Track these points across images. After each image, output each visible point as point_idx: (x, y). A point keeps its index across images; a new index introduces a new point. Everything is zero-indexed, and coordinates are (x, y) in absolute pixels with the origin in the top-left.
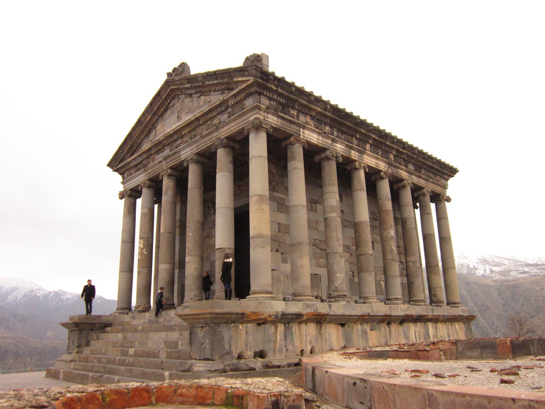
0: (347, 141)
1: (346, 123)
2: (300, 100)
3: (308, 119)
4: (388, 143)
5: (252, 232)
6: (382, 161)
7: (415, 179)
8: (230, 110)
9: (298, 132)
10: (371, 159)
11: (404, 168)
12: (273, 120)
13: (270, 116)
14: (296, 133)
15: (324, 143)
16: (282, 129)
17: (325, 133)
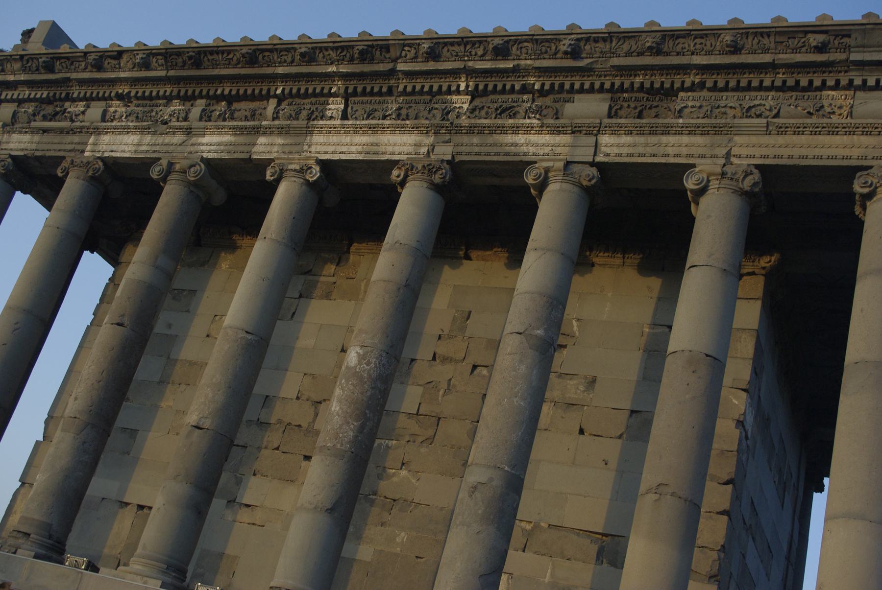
1: (216, 72)
2: (74, 76)
3: (117, 107)
4: (401, 67)
6: (402, 130)
10: (347, 139)
13: (16, 137)
15: (157, 148)
17: (165, 123)
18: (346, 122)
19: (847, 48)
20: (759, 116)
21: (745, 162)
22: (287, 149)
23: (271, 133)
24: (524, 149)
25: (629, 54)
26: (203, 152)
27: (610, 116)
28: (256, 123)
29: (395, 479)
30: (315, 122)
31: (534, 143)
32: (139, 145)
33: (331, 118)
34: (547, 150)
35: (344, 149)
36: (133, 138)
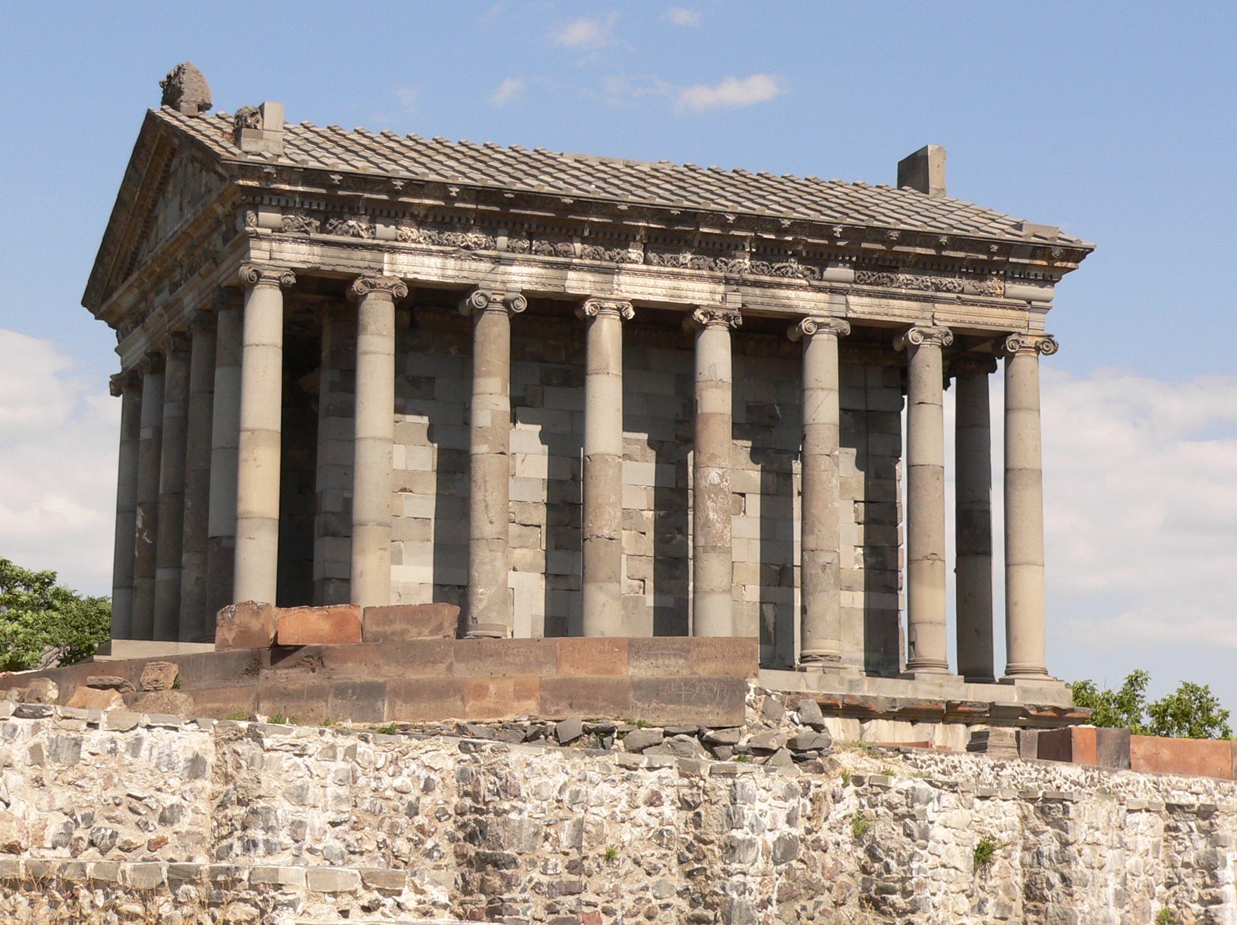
0: (550, 254)
2: (367, 195)
5: (242, 507)
6: (700, 278)
7: (862, 307)
8: (224, 228)
9: (372, 265)
10: (651, 281)
11: (804, 282)
12: (298, 254)
13: (288, 246)
15: (465, 274)
16: (323, 267)
17: (467, 247)
18: (651, 268)
21: (943, 324)
22: (599, 286)
24: (795, 302)
27: (855, 282)
28: (567, 260)
29: (674, 542)
30: (624, 265)
31: (801, 298)
32: (443, 268)
33: (637, 262)
34: (812, 304)
35: (651, 290)
36: (435, 261)
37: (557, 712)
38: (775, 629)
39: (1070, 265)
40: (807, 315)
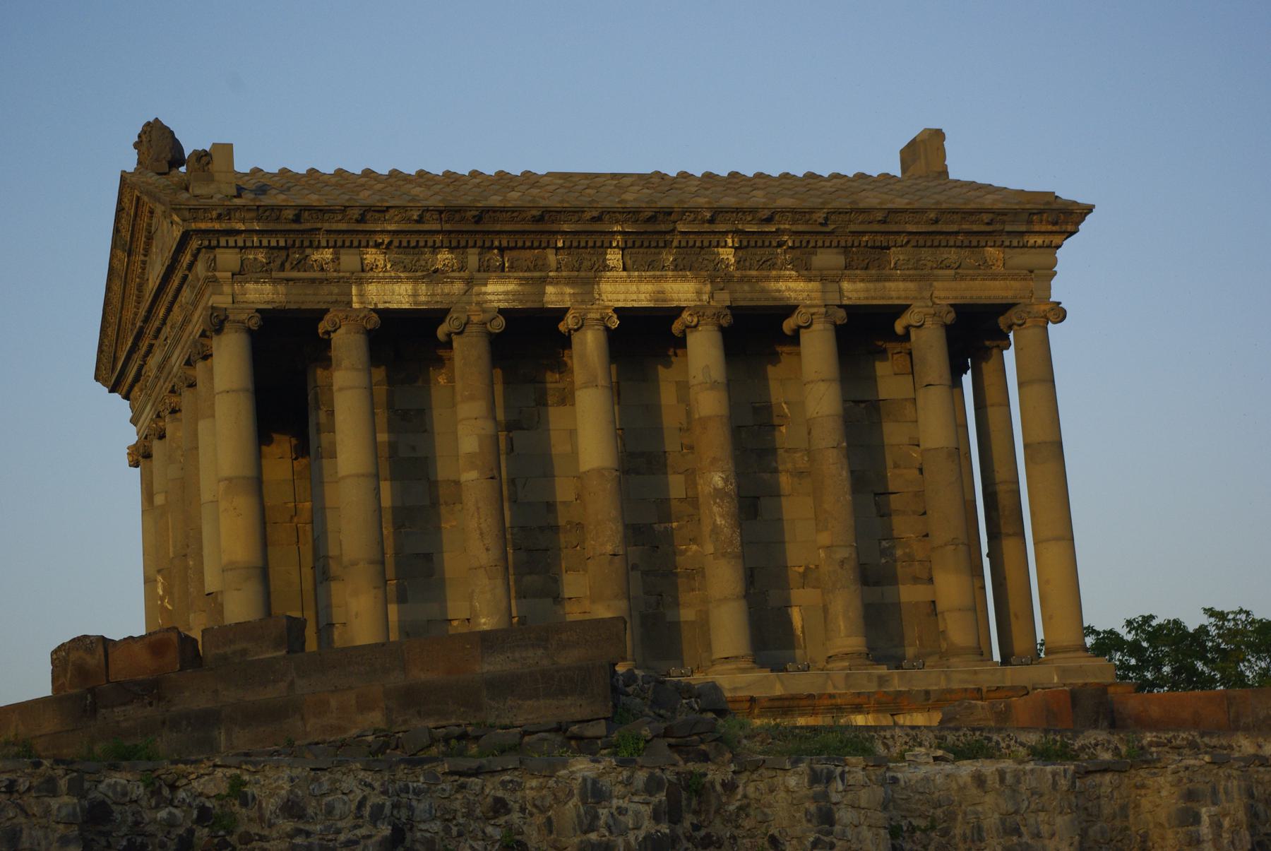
1: (498, 227)
3: (372, 256)
4: (681, 227)
6: (685, 279)
7: (855, 291)
10: (634, 288)
11: (793, 273)
12: (261, 294)
13: (250, 286)
14: (336, 302)
15: (438, 298)
17: (436, 271)
19: (1004, 222)
20: (948, 267)
23: (557, 284)
24: (787, 294)
25: (862, 222)
26: (491, 301)
29: (689, 553)
31: (791, 287)
32: (415, 295)
35: (634, 297)
37: (405, 722)
38: (803, 632)
39: (1070, 228)
40: (796, 307)
